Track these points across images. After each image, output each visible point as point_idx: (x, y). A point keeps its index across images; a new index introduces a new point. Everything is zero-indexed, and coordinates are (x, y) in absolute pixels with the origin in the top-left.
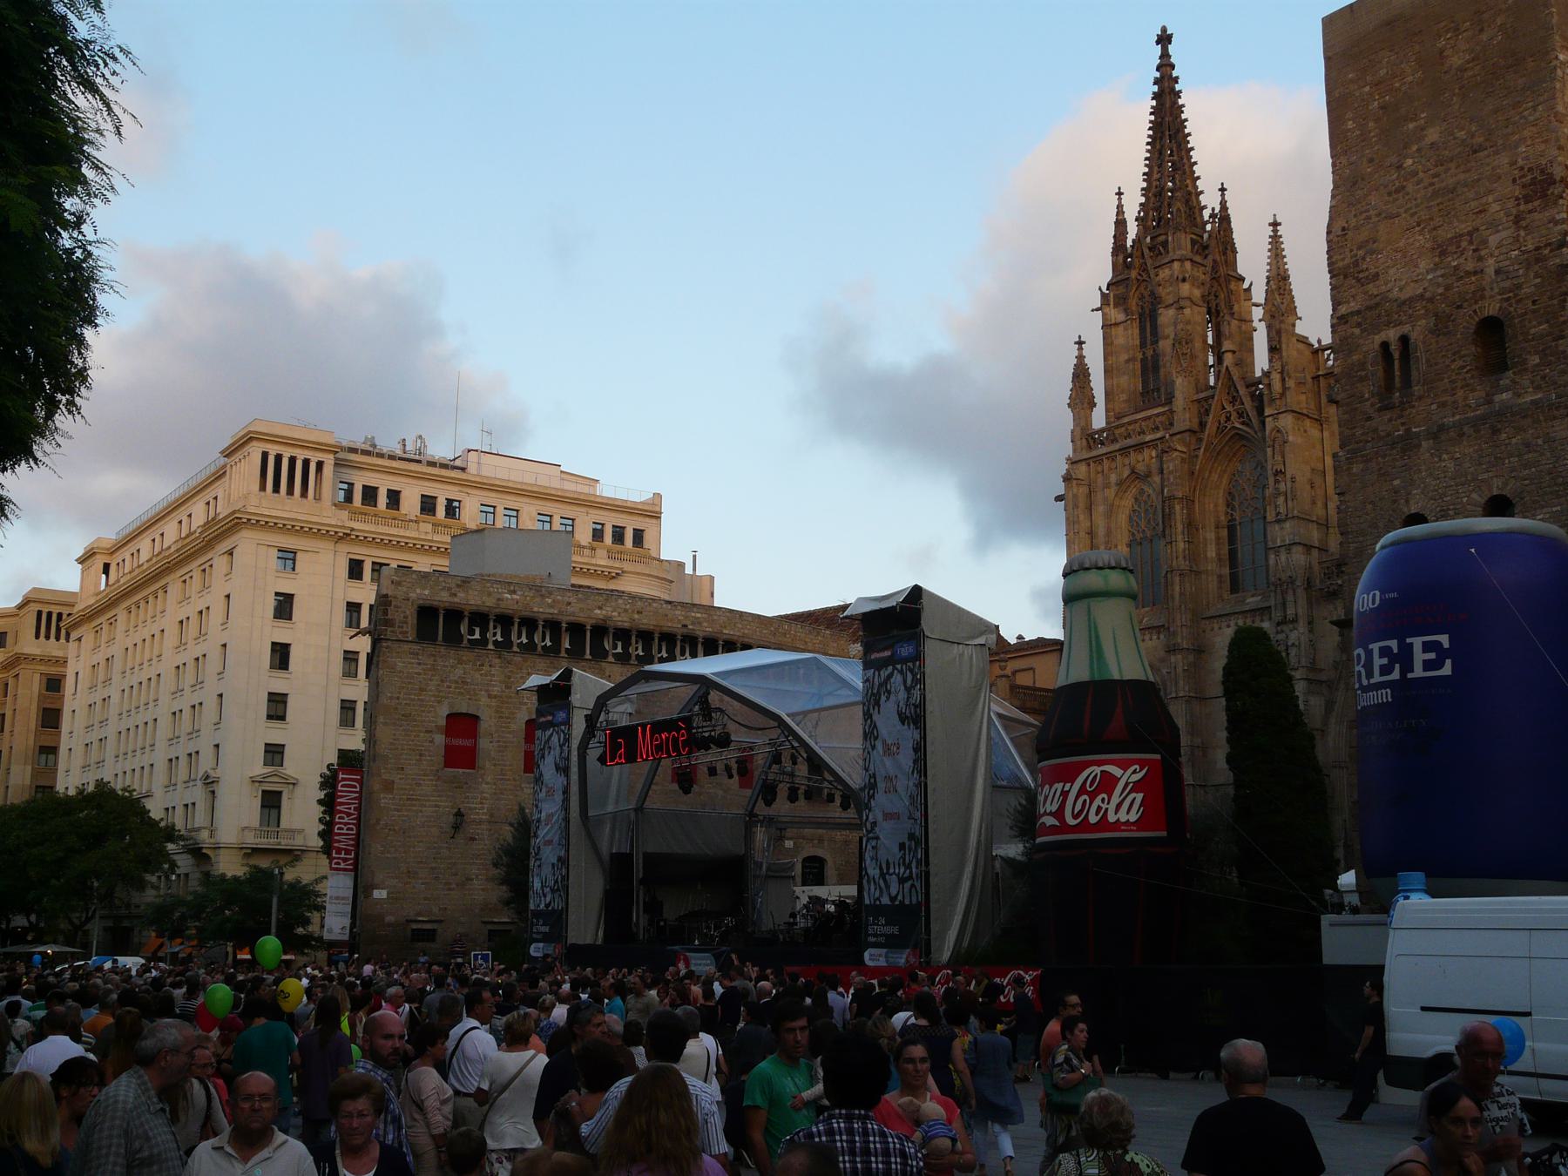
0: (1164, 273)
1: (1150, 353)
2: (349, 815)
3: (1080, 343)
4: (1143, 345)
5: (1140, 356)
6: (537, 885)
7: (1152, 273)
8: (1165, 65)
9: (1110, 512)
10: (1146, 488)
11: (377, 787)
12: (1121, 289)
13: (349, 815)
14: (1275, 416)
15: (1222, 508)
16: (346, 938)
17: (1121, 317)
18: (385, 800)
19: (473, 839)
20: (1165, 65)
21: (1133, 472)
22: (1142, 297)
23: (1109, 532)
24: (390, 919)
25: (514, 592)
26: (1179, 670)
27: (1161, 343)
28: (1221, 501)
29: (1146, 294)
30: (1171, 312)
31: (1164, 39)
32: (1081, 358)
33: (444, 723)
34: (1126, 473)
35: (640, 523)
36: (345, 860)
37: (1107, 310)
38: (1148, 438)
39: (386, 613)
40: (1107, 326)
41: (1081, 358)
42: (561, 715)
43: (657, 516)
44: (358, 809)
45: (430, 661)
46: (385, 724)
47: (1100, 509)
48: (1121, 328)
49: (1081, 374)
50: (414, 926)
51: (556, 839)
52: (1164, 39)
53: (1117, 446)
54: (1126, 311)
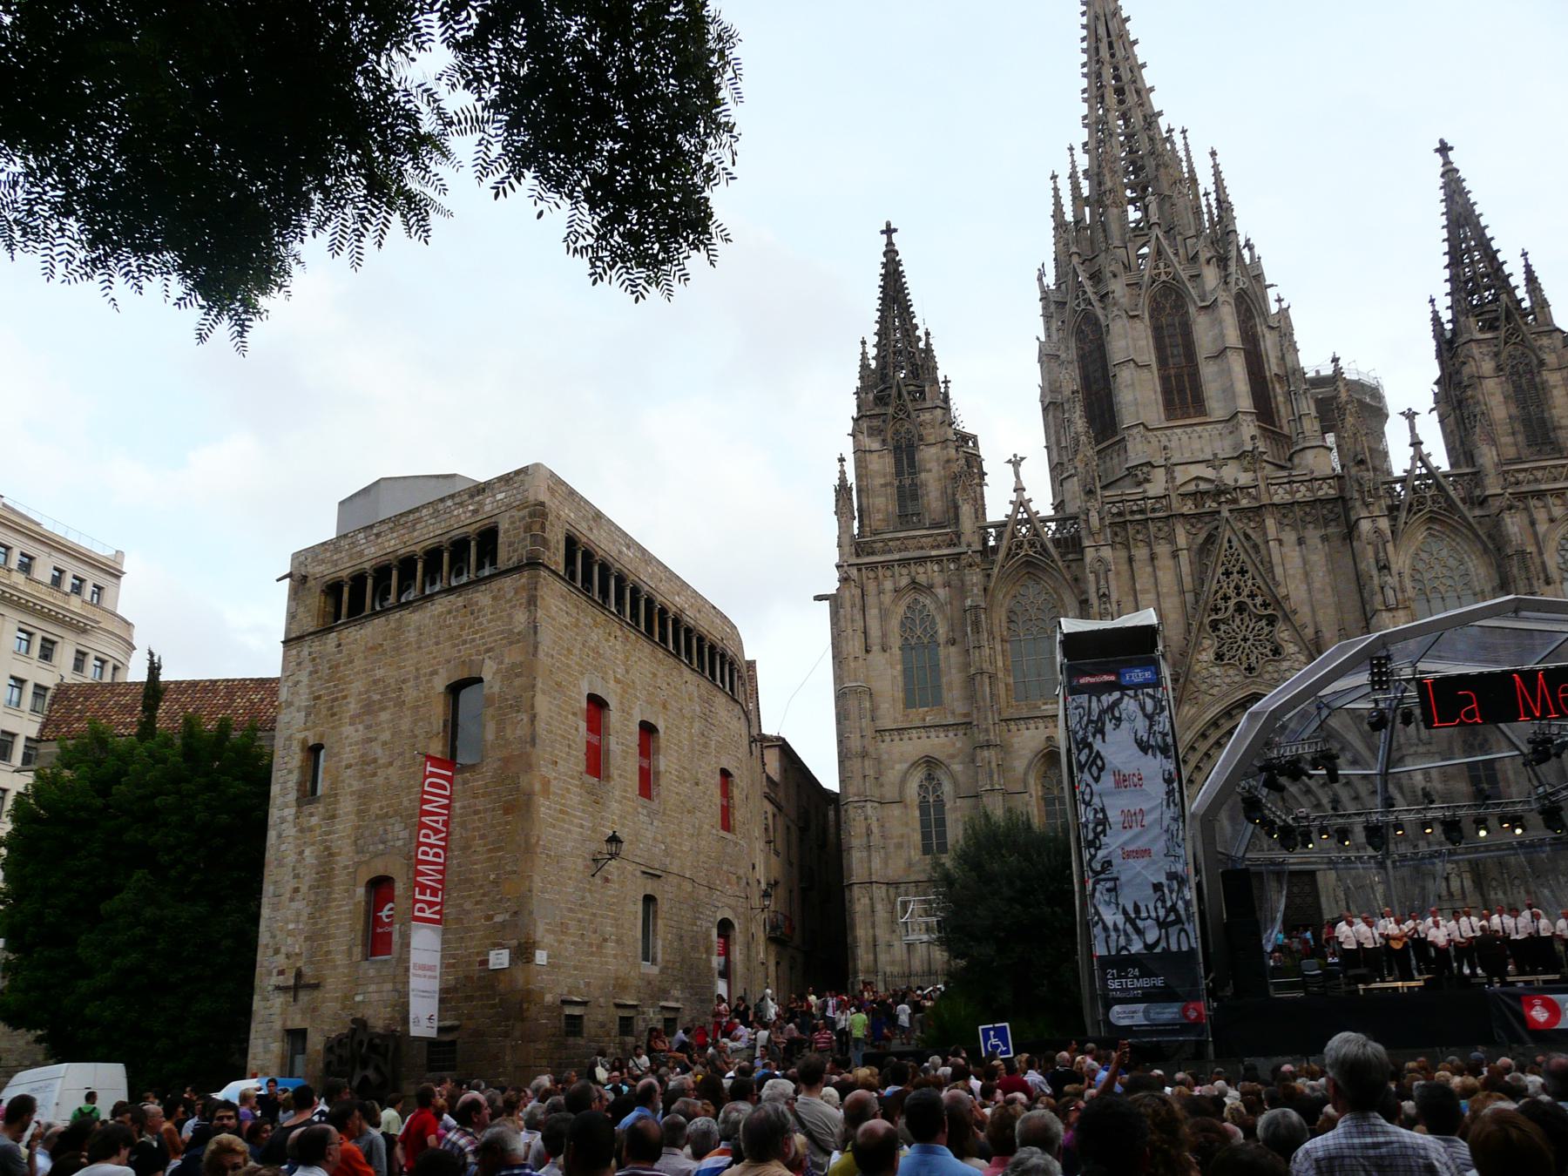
0: (926, 416)
1: (907, 482)
2: (436, 831)
3: (842, 460)
4: (899, 473)
5: (896, 483)
6: (1110, 916)
7: (914, 415)
8: (891, 252)
9: (884, 615)
10: (921, 599)
11: (537, 787)
12: (875, 423)
13: (436, 831)
14: (1097, 548)
15: (1004, 624)
16: (433, 1034)
17: (876, 446)
18: (544, 808)
19: (607, 880)
20: (891, 252)
21: (914, 582)
22: (897, 432)
23: (884, 635)
24: (548, 998)
25: (629, 548)
26: (994, 765)
27: (923, 475)
28: (1004, 618)
29: (903, 430)
30: (933, 450)
31: (889, 231)
32: (843, 473)
33: (584, 704)
34: (904, 581)
35: (102, 579)
36: (431, 904)
37: (860, 437)
38: (934, 553)
39: (543, 528)
40: (860, 452)
41: (843, 473)
42: (1138, 675)
43: (117, 575)
44: (446, 824)
45: (574, 611)
46: (544, 693)
47: (873, 612)
48: (875, 455)
49: (842, 490)
50: (568, 1011)
51: (1159, 847)
52: (889, 231)
53: (897, 556)
54: (884, 442)
